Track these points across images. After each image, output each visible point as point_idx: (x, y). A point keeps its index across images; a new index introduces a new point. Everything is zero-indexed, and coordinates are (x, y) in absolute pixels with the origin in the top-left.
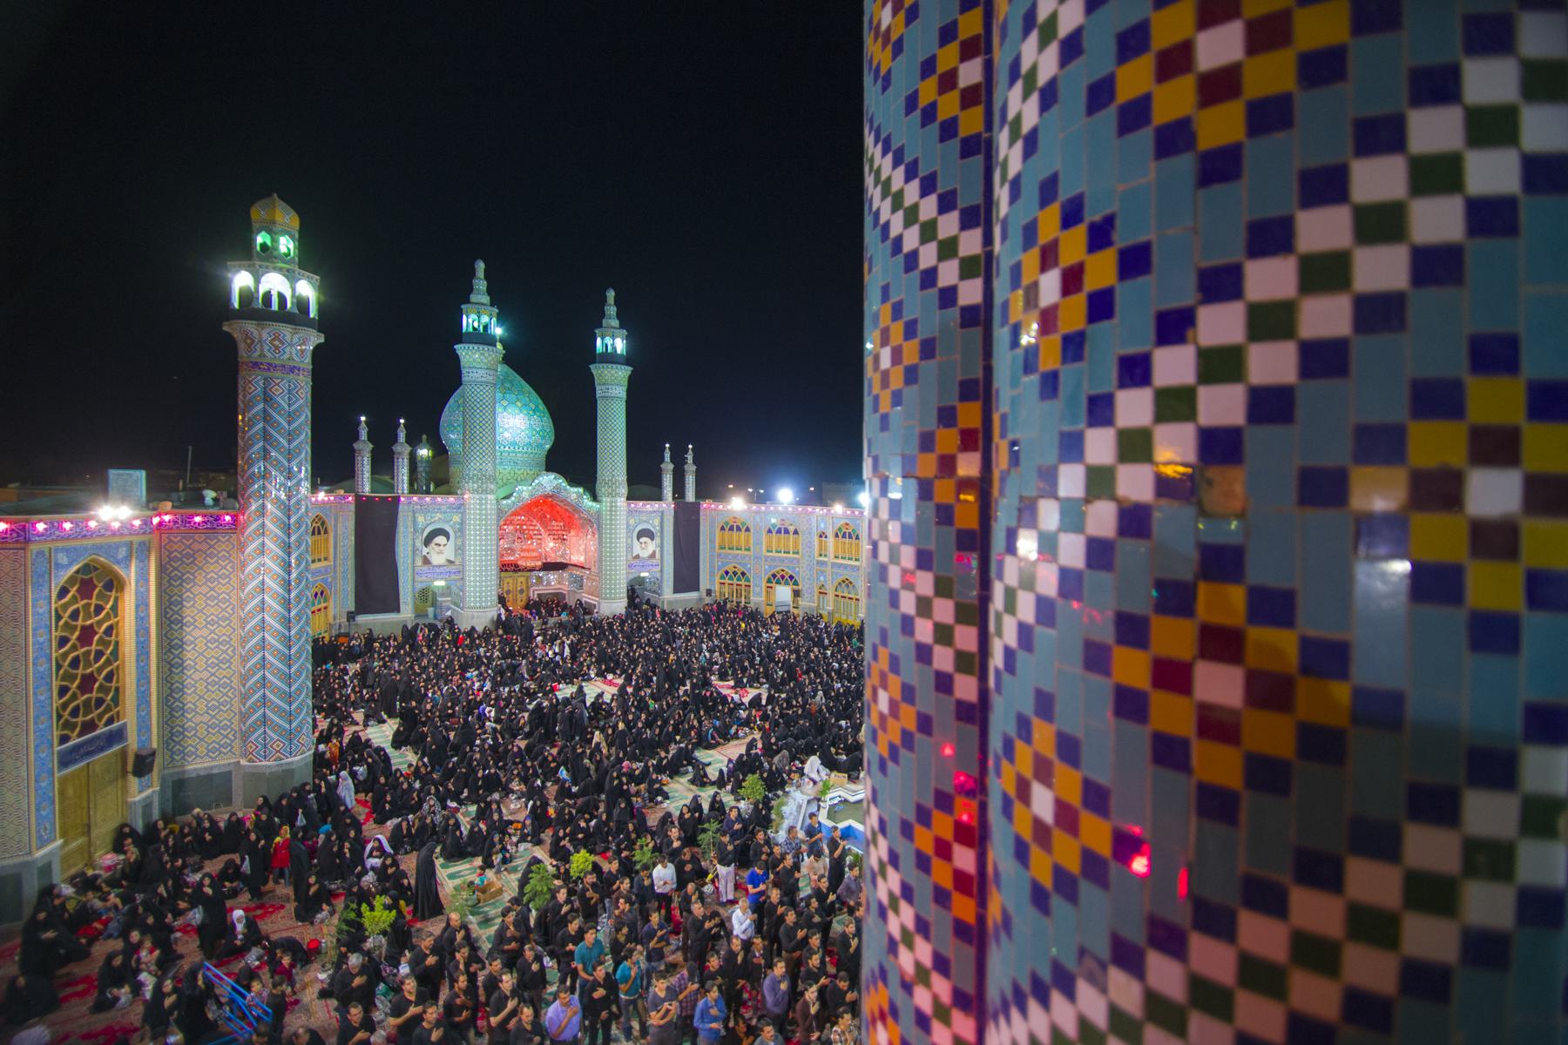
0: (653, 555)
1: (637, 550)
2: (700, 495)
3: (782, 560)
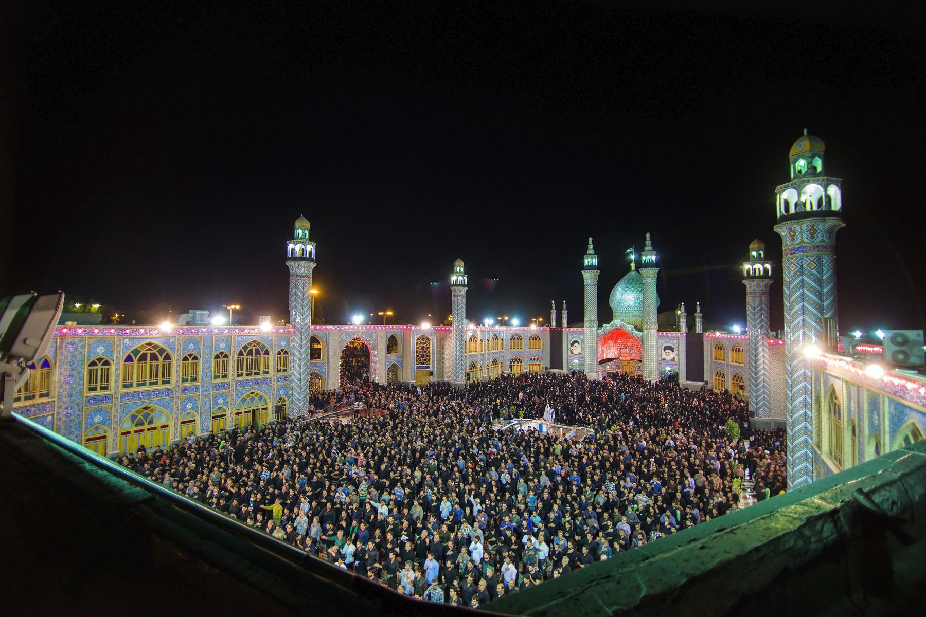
0: (674, 359)
1: (664, 355)
2: (705, 329)
3: (737, 367)
